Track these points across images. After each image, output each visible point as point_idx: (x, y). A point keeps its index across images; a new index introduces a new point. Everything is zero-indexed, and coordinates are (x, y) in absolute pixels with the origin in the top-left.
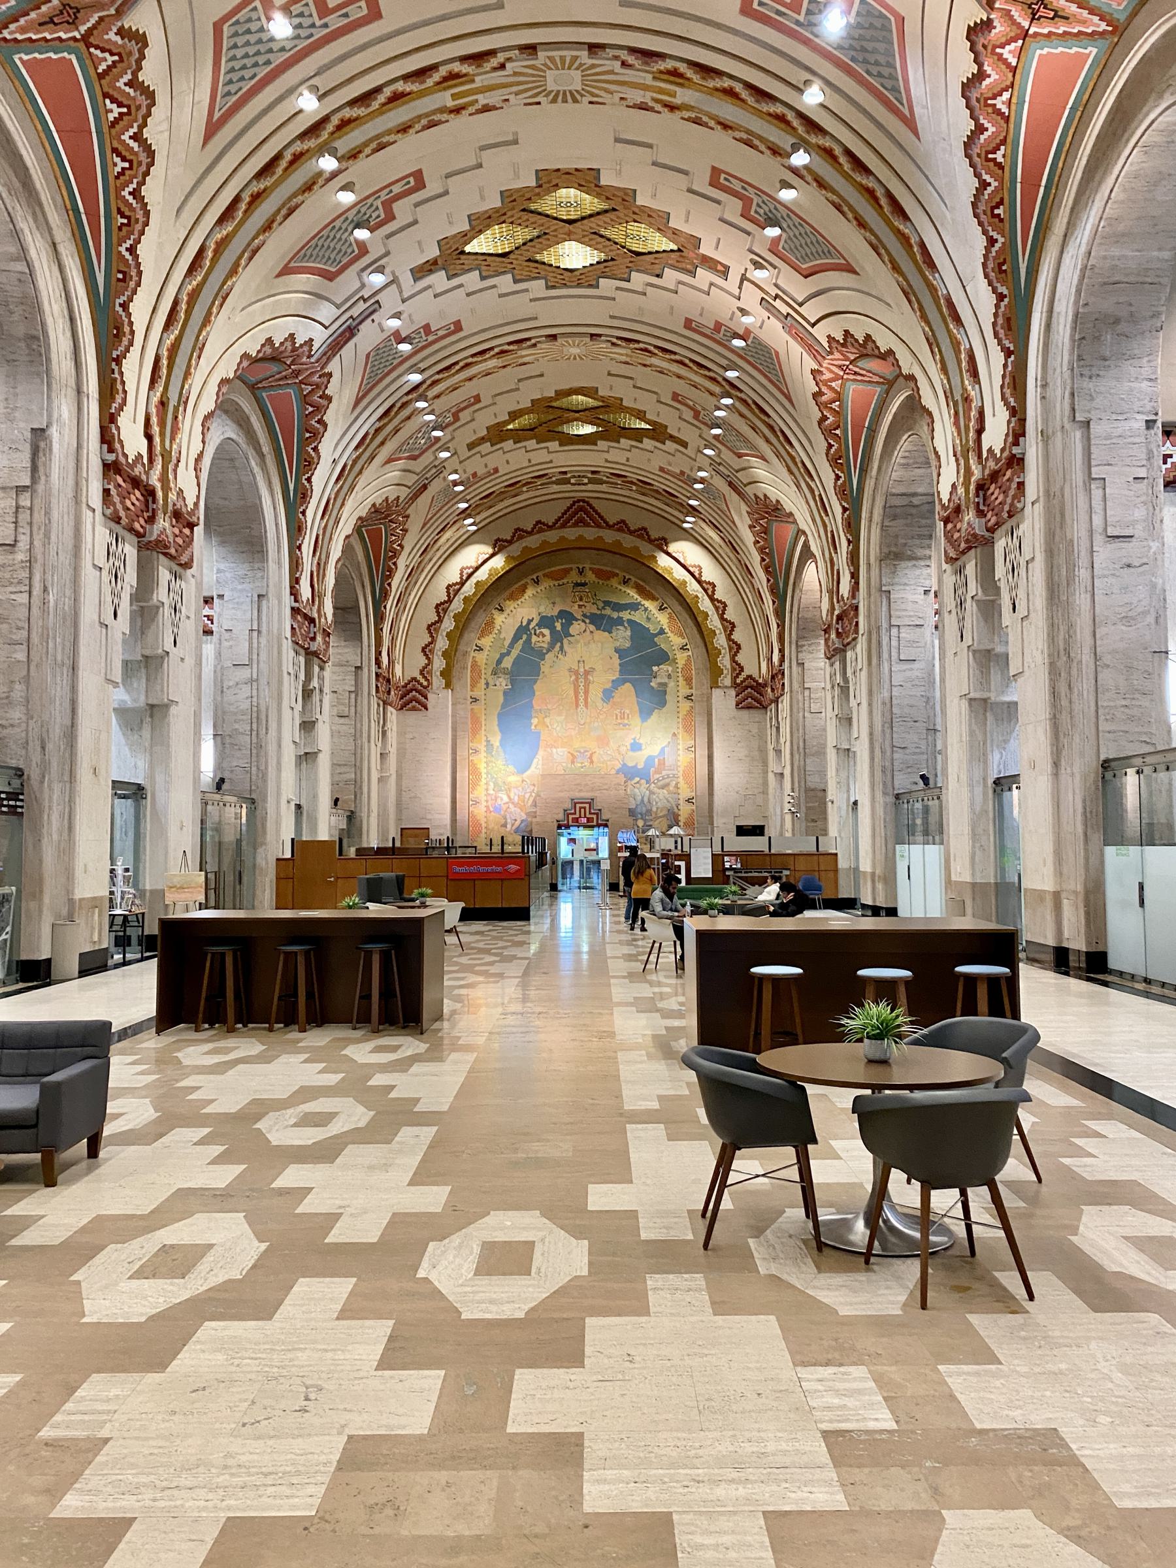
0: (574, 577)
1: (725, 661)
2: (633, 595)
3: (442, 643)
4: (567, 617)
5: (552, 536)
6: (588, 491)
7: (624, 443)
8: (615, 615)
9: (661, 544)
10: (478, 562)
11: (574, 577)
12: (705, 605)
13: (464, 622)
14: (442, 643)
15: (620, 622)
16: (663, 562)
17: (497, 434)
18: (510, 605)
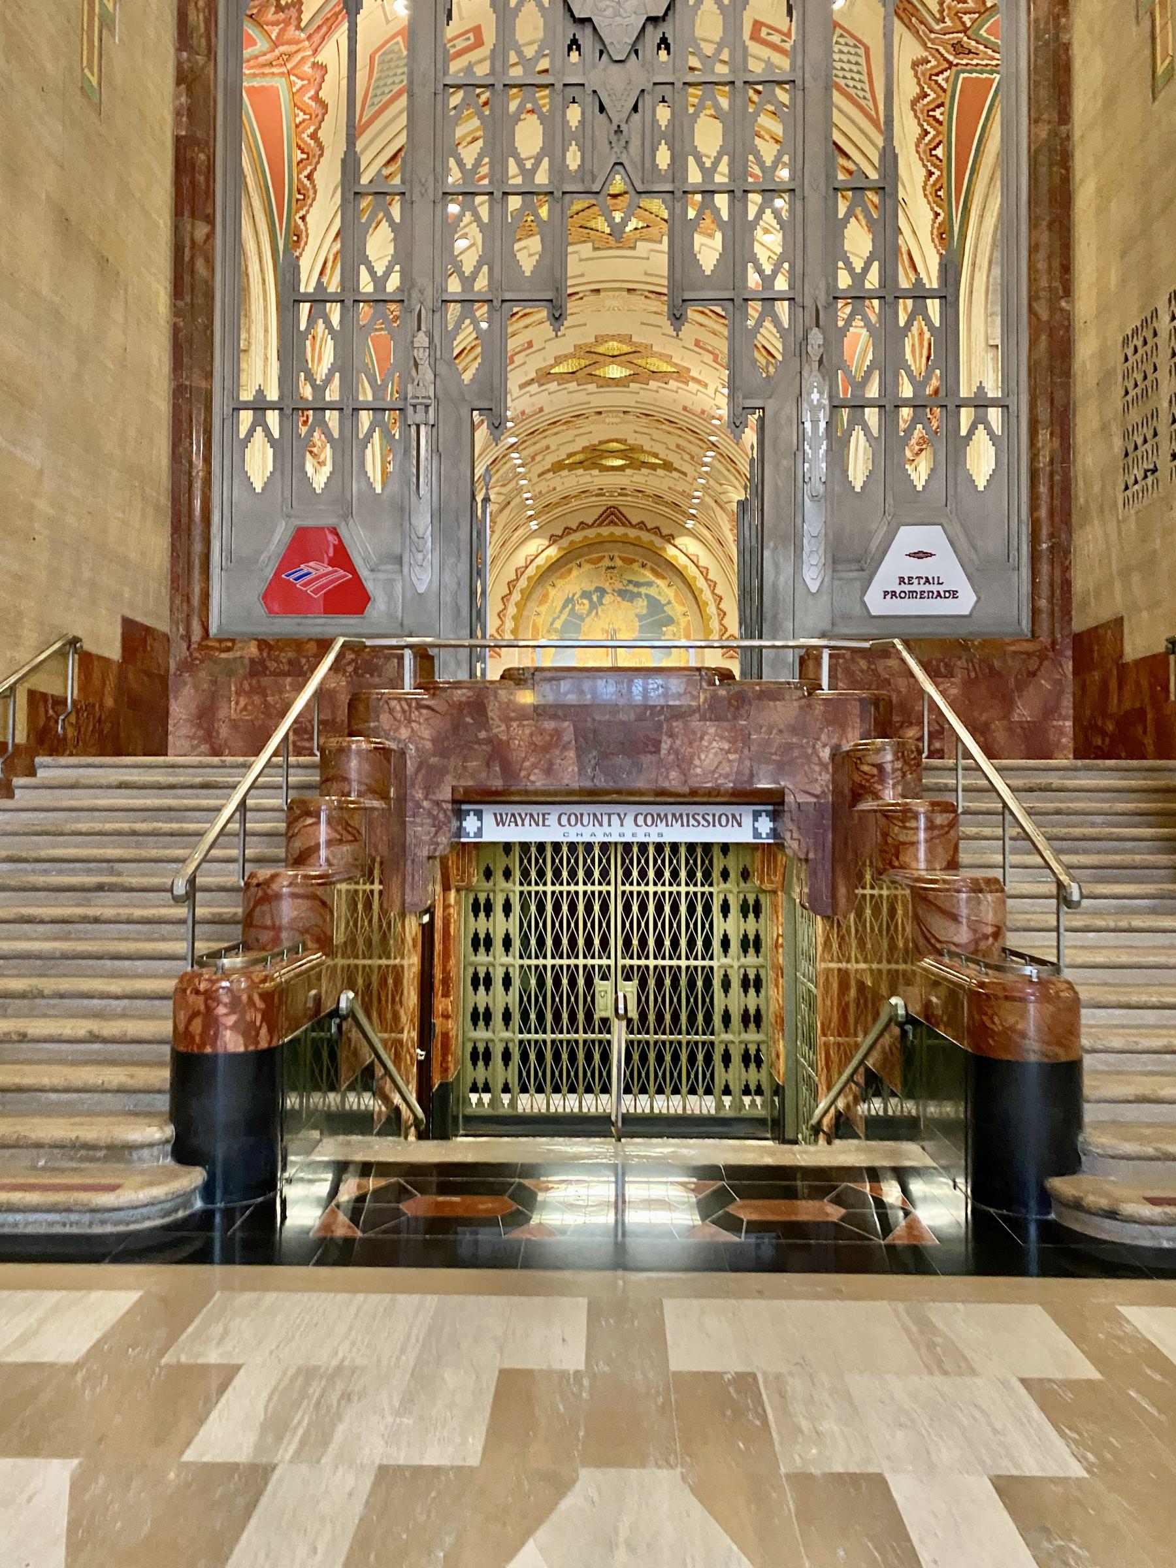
0: (606, 562)
1: (715, 624)
2: (649, 575)
3: (512, 610)
4: (601, 591)
5: (591, 533)
6: (618, 501)
7: (644, 471)
8: (636, 590)
9: (669, 538)
10: (538, 550)
11: (606, 562)
12: (701, 583)
13: (527, 595)
14: (512, 610)
15: (639, 595)
16: (671, 552)
17: (558, 467)
18: (560, 583)
